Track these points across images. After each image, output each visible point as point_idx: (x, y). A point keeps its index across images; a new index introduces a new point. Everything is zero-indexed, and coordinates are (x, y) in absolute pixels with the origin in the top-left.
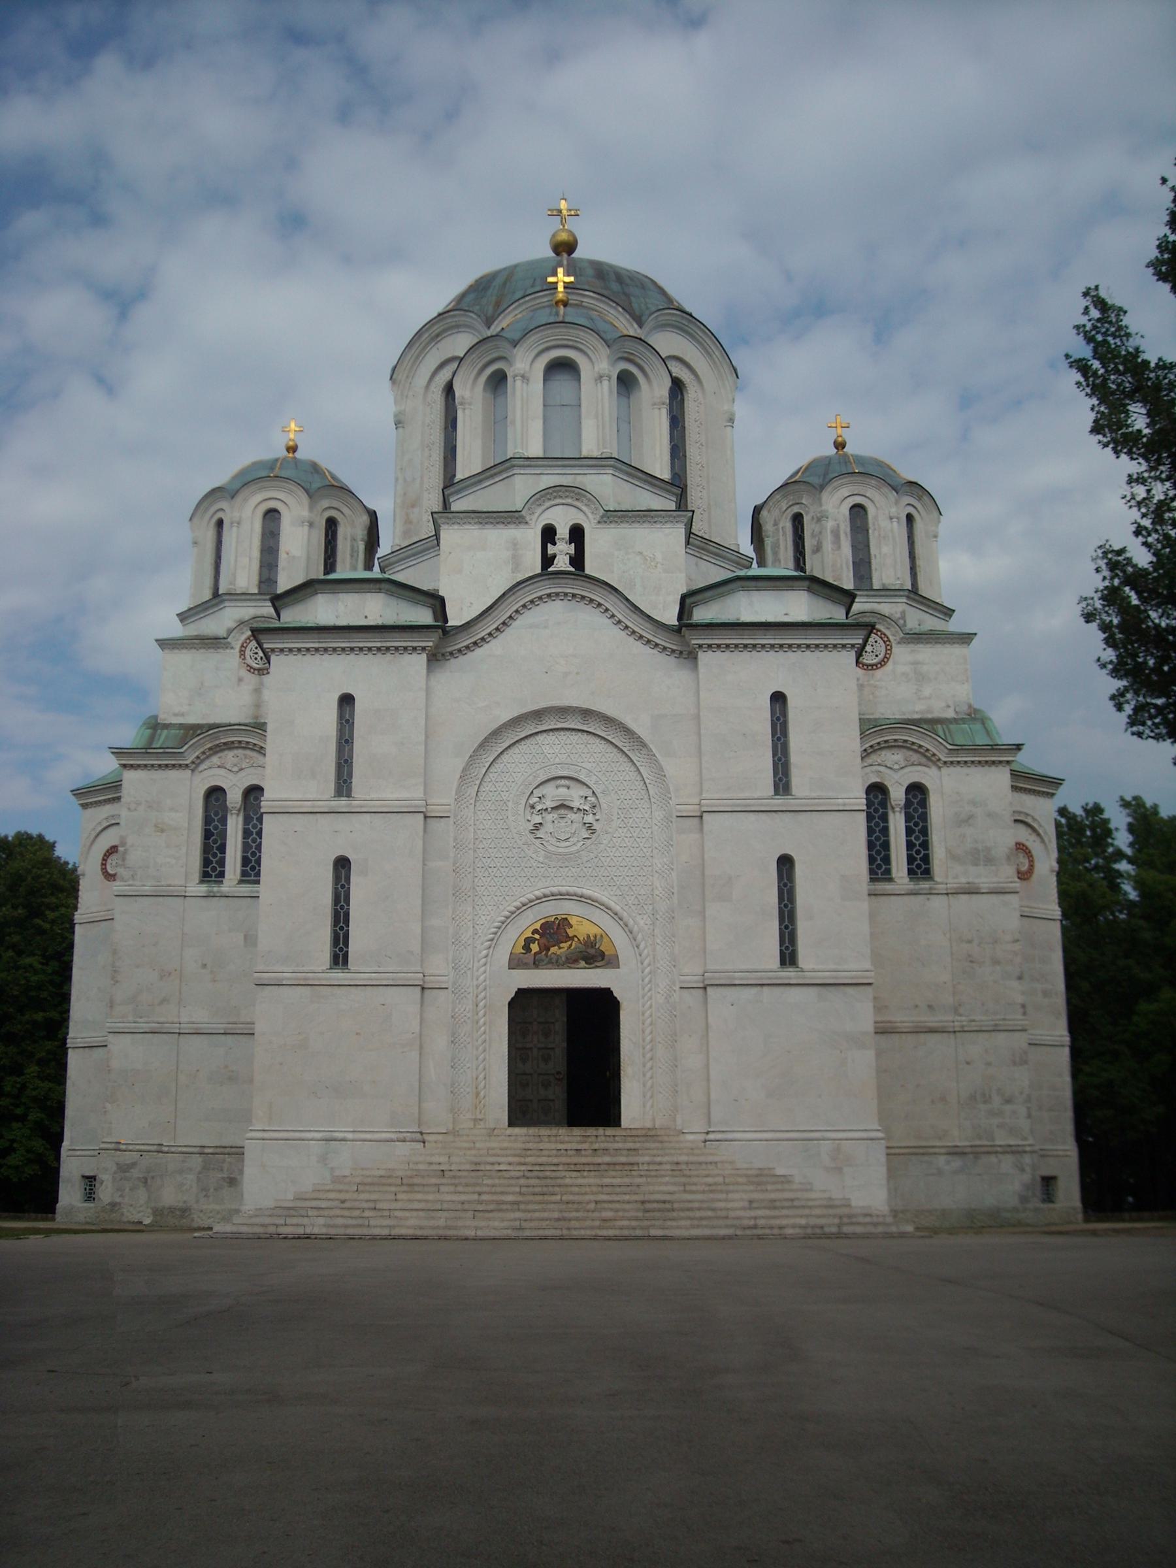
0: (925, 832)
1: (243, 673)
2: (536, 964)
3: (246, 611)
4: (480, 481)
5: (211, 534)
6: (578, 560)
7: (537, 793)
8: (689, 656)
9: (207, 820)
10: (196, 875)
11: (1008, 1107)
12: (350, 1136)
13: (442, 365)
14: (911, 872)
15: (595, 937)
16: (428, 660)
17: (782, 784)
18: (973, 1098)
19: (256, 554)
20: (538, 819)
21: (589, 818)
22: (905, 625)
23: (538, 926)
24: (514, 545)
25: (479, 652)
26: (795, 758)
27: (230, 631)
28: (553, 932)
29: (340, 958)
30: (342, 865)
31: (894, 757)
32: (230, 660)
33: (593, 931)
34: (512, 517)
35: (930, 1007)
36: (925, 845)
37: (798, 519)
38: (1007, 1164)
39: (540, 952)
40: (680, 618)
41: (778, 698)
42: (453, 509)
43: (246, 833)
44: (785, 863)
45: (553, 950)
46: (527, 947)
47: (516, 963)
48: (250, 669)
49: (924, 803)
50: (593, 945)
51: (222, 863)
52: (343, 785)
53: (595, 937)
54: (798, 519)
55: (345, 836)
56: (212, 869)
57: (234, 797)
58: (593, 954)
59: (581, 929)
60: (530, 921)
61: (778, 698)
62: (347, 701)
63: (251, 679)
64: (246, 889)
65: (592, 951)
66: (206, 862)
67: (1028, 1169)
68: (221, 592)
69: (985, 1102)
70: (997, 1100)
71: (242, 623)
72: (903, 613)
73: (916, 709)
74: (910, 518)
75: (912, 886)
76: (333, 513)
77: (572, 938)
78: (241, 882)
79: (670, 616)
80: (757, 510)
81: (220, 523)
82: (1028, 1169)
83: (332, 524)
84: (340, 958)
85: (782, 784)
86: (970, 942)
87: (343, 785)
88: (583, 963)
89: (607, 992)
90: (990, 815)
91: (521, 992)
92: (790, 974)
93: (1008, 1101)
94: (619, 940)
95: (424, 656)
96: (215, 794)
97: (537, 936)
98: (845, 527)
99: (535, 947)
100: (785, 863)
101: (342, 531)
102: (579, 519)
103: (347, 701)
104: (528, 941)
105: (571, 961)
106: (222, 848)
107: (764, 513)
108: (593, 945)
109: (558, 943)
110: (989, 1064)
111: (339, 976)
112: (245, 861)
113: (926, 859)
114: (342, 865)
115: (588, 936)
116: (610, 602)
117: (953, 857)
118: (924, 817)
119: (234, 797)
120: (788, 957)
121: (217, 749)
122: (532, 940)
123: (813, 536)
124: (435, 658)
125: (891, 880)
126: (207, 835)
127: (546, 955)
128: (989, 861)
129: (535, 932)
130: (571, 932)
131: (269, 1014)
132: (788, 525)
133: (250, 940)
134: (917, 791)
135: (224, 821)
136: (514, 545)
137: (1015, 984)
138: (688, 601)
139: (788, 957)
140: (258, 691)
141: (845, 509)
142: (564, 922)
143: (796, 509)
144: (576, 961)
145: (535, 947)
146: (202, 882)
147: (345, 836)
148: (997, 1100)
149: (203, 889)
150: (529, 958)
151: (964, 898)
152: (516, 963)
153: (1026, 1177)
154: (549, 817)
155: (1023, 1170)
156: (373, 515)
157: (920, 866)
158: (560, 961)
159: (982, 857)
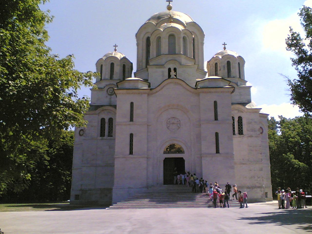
0: (242, 125)
1: (107, 95)
2: (169, 153)
3: (108, 83)
4: (156, 59)
5: (100, 68)
6: (176, 76)
7: (169, 120)
8: (198, 94)
9: (101, 125)
10: (99, 135)
11: (259, 179)
12: (133, 187)
13: (146, 33)
14: (239, 134)
15: (180, 148)
16: (148, 95)
17: (216, 119)
18: (252, 177)
19: (109, 72)
20: (169, 125)
21: (179, 125)
22: (238, 84)
23: (169, 146)
24: (163, 72)
25: (157, 94)
26: (219, 113)
27: (104, 87)
28: (172, 147)
29: (131, 153)
30: (131, 136)
31: (236, 112)
32: (105, 92)
33: (179, 147)
34: (162, 66)
35: (243, 159)
36: (242, 128)
37: (216, 64)
38: (258, 190)
40: (196, 86)
41: (215, 103)
42: (150, 65)
43: (109, 127)
44: (217, 134)
45: (172, 150)
46: (167, 150)
47: (165, 153)
48: (109, 94)
49: (241, 120)
51: (104, 133)
52: (131, 119)
54: (216, 64)
55: (133, 129)
56: (102, 134)
57: (107, 121)
58: (180, 151)
59: (177, 146)
60: (168, 145)
61: (215, 103)
62: (132, 104)
63: (109, 97)
64: (109, 138)
66: (101, 133)
67: (263, 191)
68: (102, 79)
69: (254, 178)
70: (256, 178)
71: (107, 85)
72: (237, 82)
73: (240, 101)
74: (239, 63)
75: (239, 136)
76: (124, 63)
77: (176, 148)
78: (108, 136)
79: (194, 86)
80: (208, 62)
81: (102, 66)
82: (263, 191)
83: (124, 66)
84: (131, 153)
85: (216, 119)
86: (251, 147)
87: (131, 119)
88: (178, 153)
89: (182, 158)
90: (255, 122)
91: (166, 158)
92: (218, 154)
93: (259, 178)
94: (185, 149)
95: (147, 95)
96: (103, 120)
97: (169, 148)
98: (226, 66)
99: (168, 150)
100: (217, 134)
101: (126, 67)
102: (175, 67)
103: (132, 104)
104: (167, 148)
105: (175, 152)
106: (104, 130)
107: (210, 62)
109: (173, 149)
110: (255, 170)
111: (131, 156)
112: (109, 132)
113: (242, 131)
114: (131, 136)
115: (179, 147)
116: (183, 83)
117: (248, 130)
118: (242, 122)
119: (107, 121)
120: (218, 152)
121: (103, 110)
122: (168, 148)
123: (220, 67)
124: (148, 95)
125: (235, 135)
126: (101, 127)
128: (255, 131)
129: (168, 147)
130: (175, 147)
131: (118, 164)
132: (214, 65)
133: (112, 147)
134: (240, 119)
135: (105, 125)
136: (163, 72)
137: (260, 155)
138: (197, 83)
139: (218, 152)
140: (110, 98)
141: (226, 62)
142: (174, 145)
143: (216, 62)
145: (168, 150)
146: (101, 136)
147: (133, 129)
148: (256, 178)
149: (101, 138)
150: (167, 152)
151: (250, 138)
152: (165, 153)
153: (262, 193)
154: (171, 125)
155: (262, 191)
156: (132, 63)
157: (241, 132)
159: (253, 130)
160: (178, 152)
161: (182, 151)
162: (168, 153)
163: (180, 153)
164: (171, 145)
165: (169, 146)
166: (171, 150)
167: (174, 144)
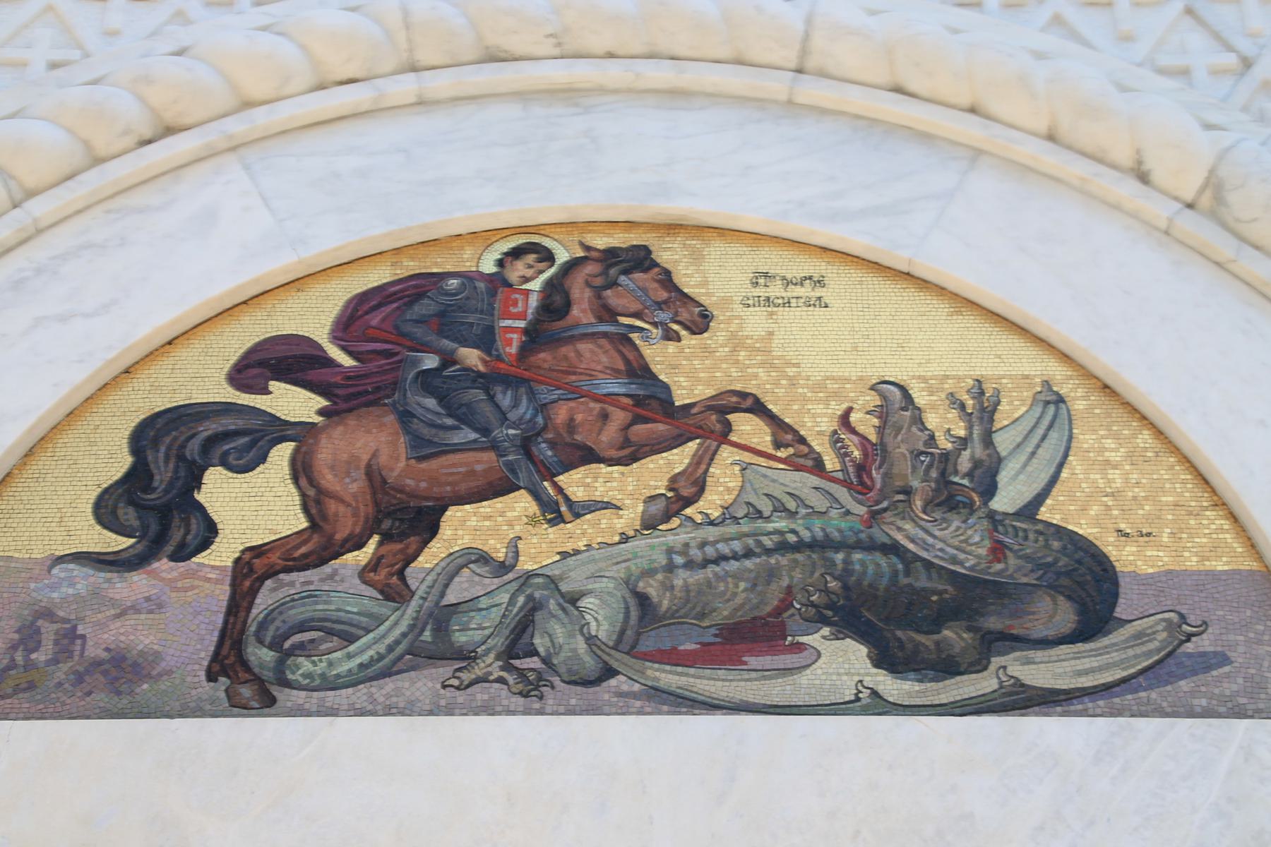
23: (313, 317)
39: (317, 546)
46: (156, 501)
50: (960, 484)
53: (982, 408)
65: (956, 544)
88: (842, 661)
97: (292, 402)
108: (960, 484)
109: (536, 463)
115: (896, 403)
122: (245, 442)
127: (390, 583)
130: (687, 370)
144: (754, 635)
145: (252, 506)
158: (554, 634)
160: (851, 614)
161: (1126, 558)
162: (228, 661)
163: (1041, 671)
164: (417, 288)
165: (313, 317)
166: (413, 520)
167: (640, 259)
